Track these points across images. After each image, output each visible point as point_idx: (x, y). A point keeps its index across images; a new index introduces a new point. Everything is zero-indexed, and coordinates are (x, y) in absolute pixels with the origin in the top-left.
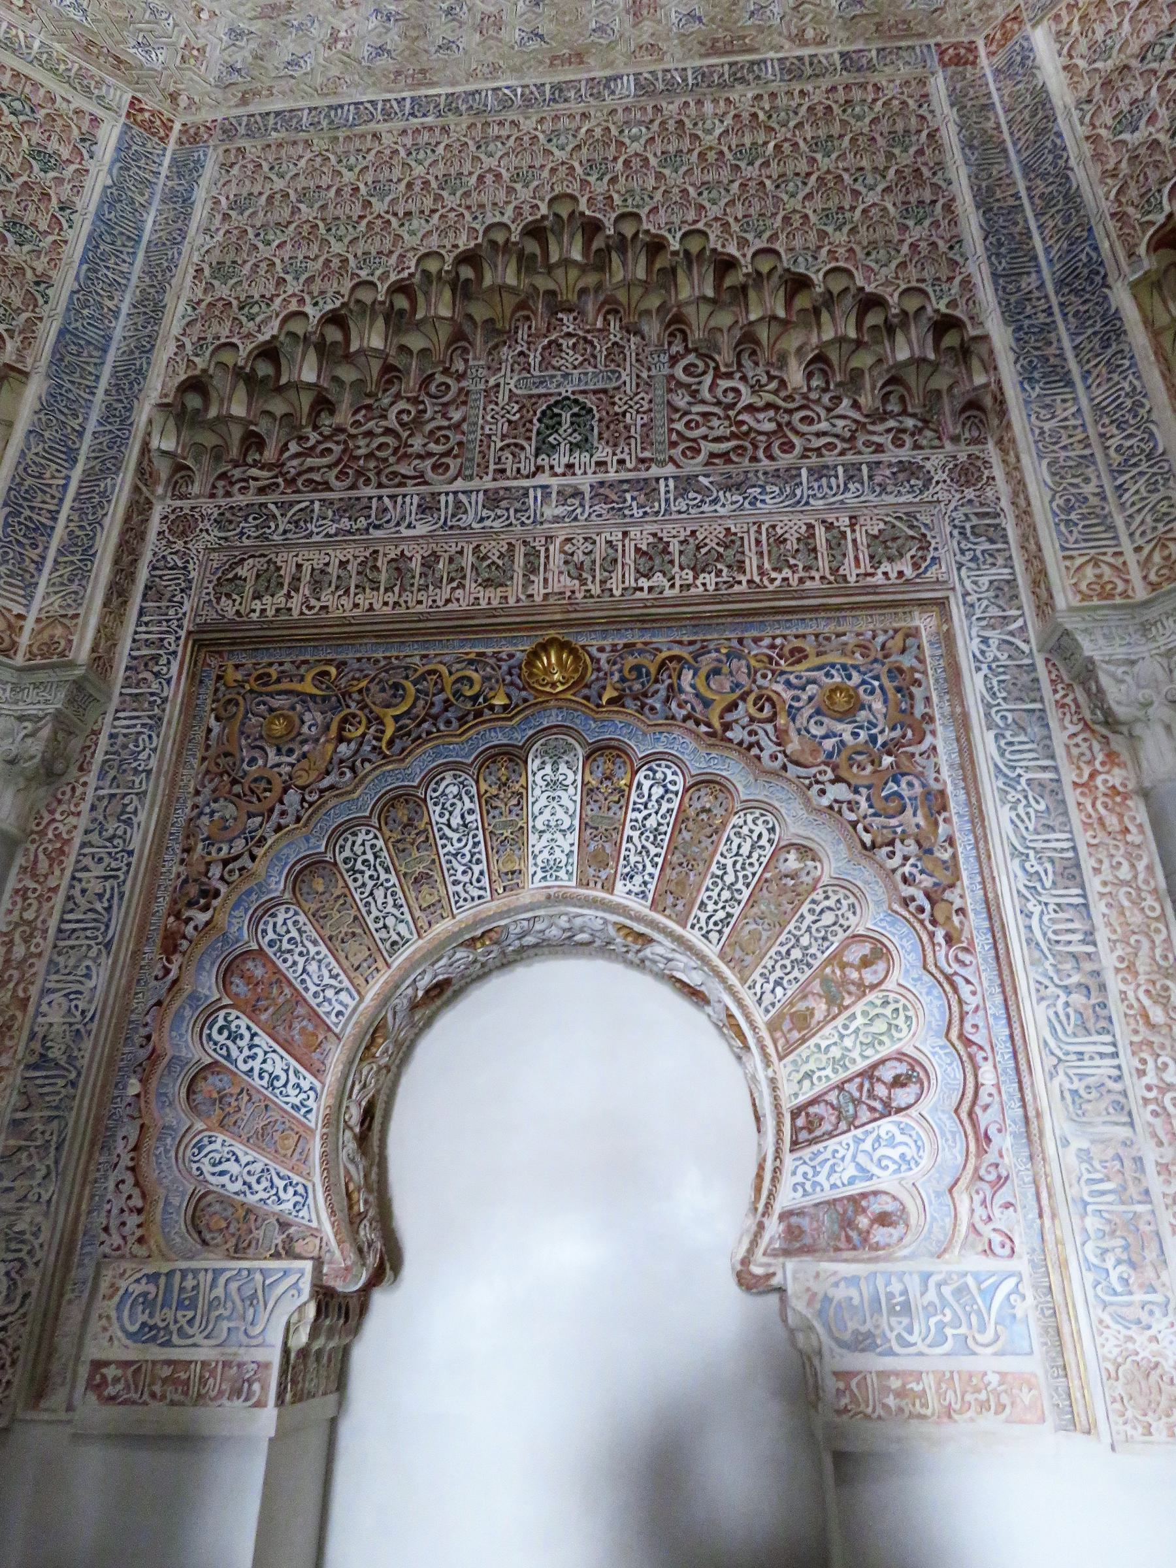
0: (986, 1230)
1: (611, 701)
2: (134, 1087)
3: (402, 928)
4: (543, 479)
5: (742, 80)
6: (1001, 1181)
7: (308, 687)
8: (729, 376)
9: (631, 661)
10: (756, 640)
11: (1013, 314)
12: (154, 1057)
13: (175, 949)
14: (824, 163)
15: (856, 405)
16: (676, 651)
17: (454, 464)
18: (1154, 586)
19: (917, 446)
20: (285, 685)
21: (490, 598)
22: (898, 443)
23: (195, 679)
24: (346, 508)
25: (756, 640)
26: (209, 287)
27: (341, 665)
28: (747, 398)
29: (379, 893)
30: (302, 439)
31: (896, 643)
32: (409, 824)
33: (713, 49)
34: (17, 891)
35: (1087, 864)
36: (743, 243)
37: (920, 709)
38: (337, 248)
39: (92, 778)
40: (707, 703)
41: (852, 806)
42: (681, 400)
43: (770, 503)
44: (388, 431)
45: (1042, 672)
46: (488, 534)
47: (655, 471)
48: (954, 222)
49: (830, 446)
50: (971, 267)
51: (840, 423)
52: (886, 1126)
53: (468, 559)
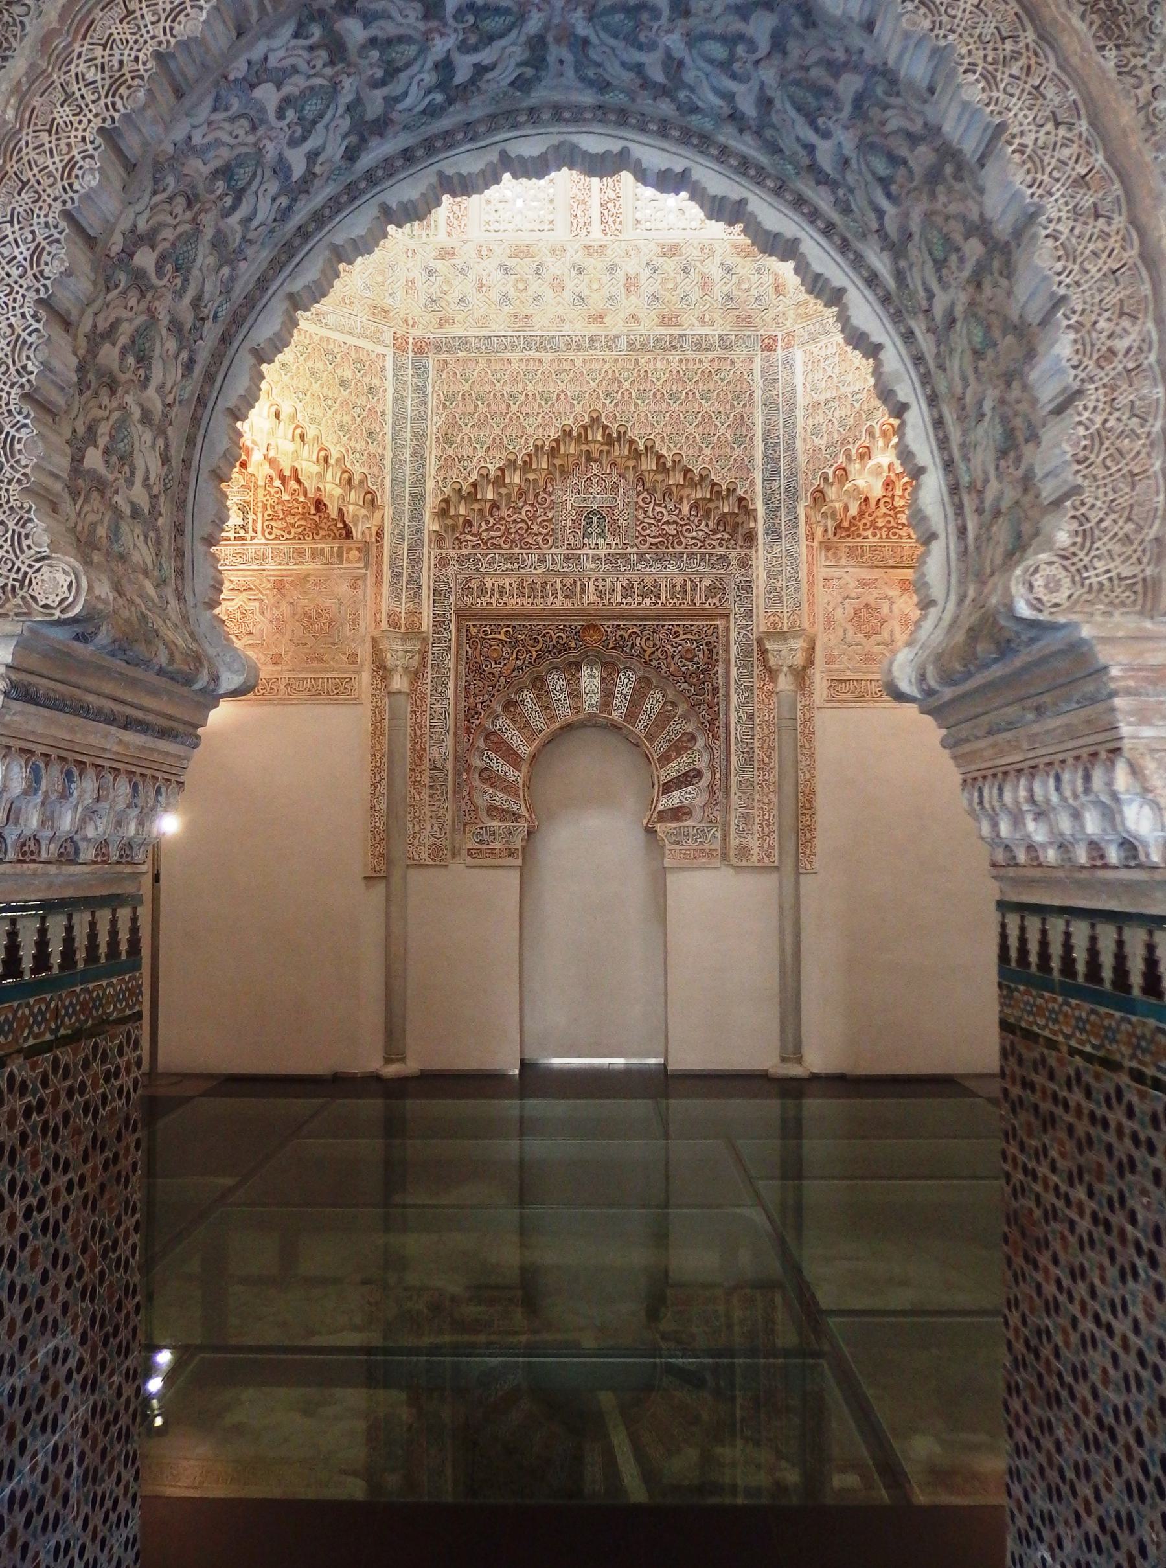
2: (465, 776)
4: (586, 550)
5: (674, 347)
11: (767, 500)
12: (470, 767)
14: (706, 407)
21: (567, 603)
23: (457, 629)
24: (511, 558)
30: (487, 522)
31: (709, 632)
33: (663, 324)
38: (498, 431)
39: (429, 669)
43: (672, 569)
46: (565, 574)
47: (629, 550)
48: (753, 448)
50: (755, 475)
53: (559, 586)
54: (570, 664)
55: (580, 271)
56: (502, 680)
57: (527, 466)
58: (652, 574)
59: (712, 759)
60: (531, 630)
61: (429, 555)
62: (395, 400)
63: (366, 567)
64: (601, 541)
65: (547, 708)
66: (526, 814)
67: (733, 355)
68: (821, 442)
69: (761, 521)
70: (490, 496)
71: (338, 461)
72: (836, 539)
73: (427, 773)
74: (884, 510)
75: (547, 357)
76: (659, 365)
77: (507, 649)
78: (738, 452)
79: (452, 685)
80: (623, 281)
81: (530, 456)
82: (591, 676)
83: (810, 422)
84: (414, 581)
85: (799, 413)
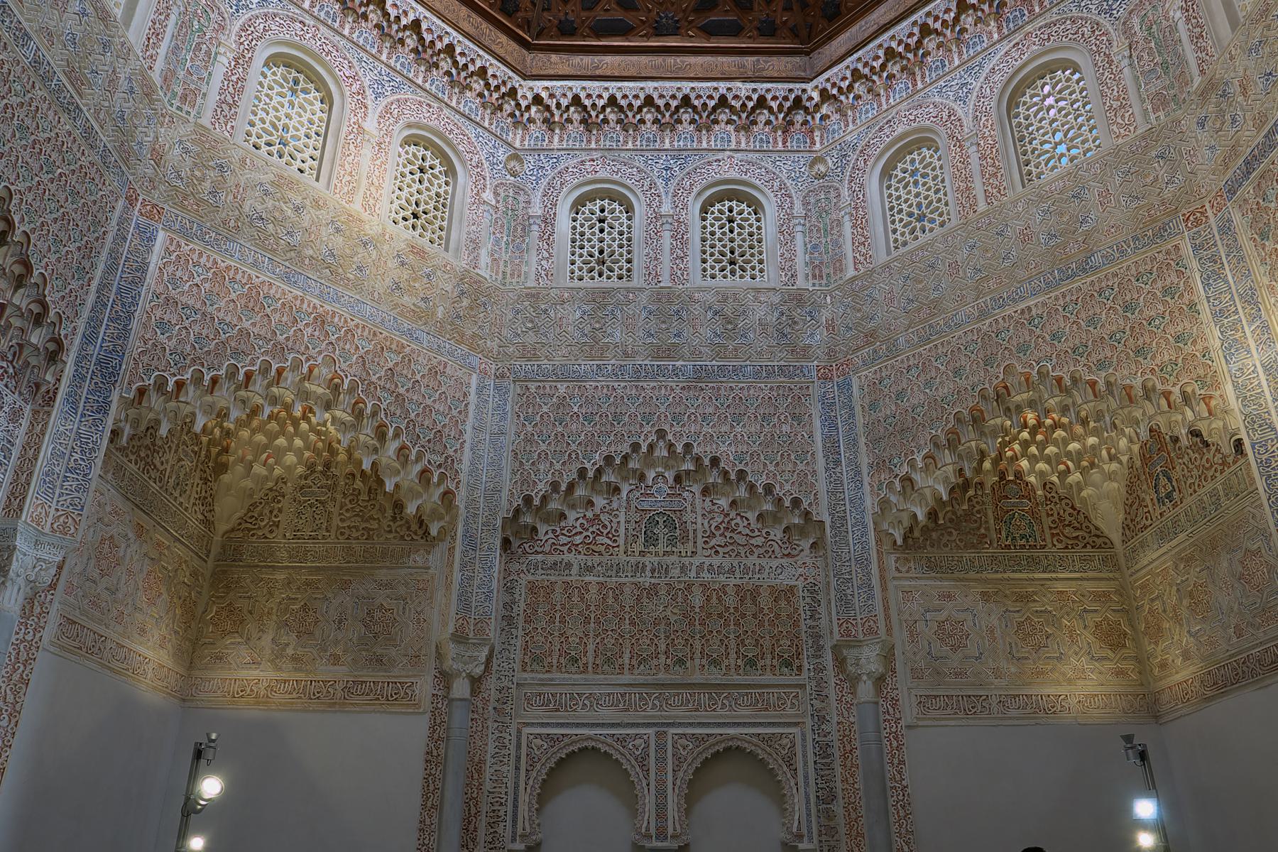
18: (53, 531)
78: (74, 285)
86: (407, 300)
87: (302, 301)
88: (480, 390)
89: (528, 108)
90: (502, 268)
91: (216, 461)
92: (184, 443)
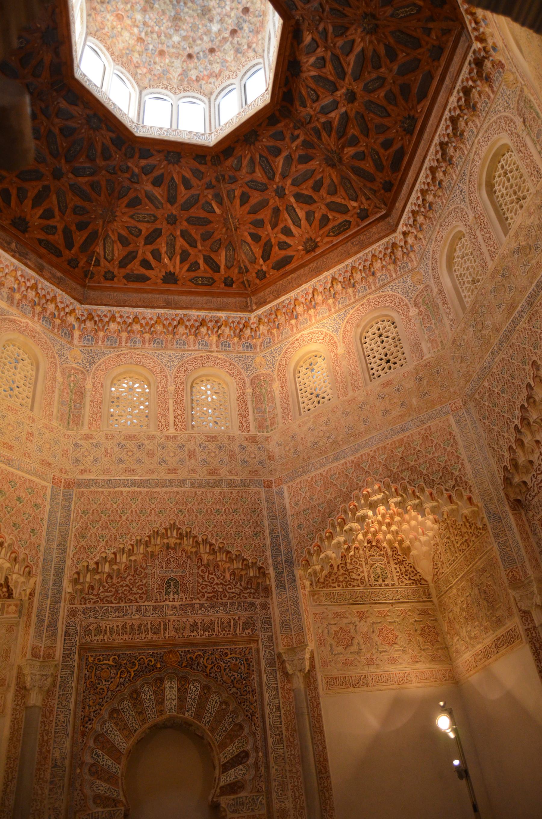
0: (258, 787)
1: (185, 666)
3: (137, 726)
4: (167, 603)
5: (217, 486)
6: (261, 776)
7: (111, 663)
8: (212, 574)
9: (189, 656)
10: (217, 650)
11: (275, 567)
12: (83, 763)
13: (85, 735)
15: (241, 585)
16: (199, 653)
17: (144, 596)
18: (297, 645)
19: (254, 598)
20: (105, 662)
22: (250, 597)
23: (80, 659)
24: (117, 609)
25: (217, 650)
26: (79, 542)
27: (119, 656)
28: (216, 581)
29: (131, 717)
31: (247, 652)
32: (136, 699)
34: (42, 722)
35: (282, 706)
36: (216, 540)
37: (251, 668)
38: (113, 531)
39: (57, 689)
40: (206, 667)
41: (237, 693)
42: (201, 581)
43: (221, 612)
44: (127, 585)
45: (276, 660)
47: (194, 602)
49: (235, 597)
51: (237, 590)
52: (241, 767)
53: (149, 626)
54: (156, 680)
55: (163, 448)
56: (110, 693)
57: (131, 552)
58: (210, 615)
59: (255, 741)
60: (131, 657)
61: (64, 608)
62: (50, 512)
63: (20, 616)
64: (176, 596)
65: (140, 713)
66: (122, 798)
67: (249, 490)
68: (304, 532)
69: (273, 580)
70: (107, 569)
71: (9, 545)
72: (318, 589)
73: (49, 771)
74: (342, 571)
75: (144, 490)
76: (208, 495)
77: (114, 671)
78: (256, 541)
79: (73, 700)
80: (186, 453)
81: (133, 545)
82: (171, 687)
83: (296, 522)
84: (53, 625)
85: (289, 518)
86: (395, 413)
87: (346, 463)
88: (458, 422)
89: (406, 242)
90: (439, 340)
91: (403, 549)
92: (371, 556)
